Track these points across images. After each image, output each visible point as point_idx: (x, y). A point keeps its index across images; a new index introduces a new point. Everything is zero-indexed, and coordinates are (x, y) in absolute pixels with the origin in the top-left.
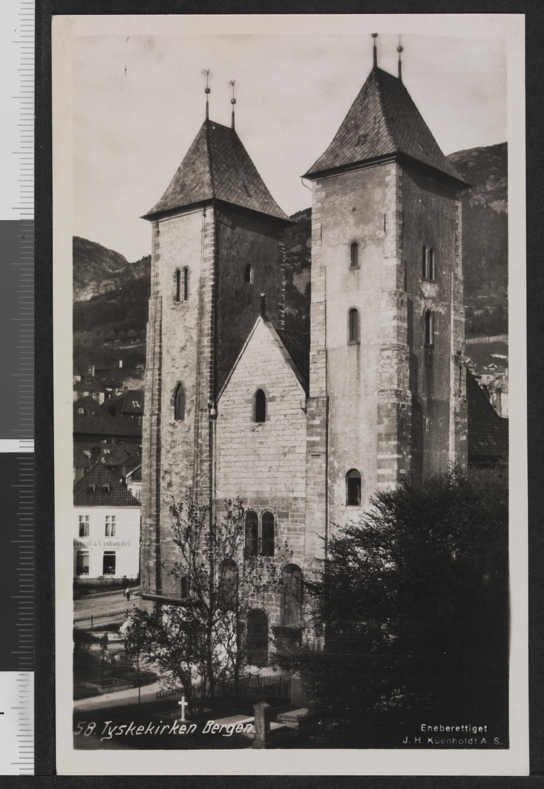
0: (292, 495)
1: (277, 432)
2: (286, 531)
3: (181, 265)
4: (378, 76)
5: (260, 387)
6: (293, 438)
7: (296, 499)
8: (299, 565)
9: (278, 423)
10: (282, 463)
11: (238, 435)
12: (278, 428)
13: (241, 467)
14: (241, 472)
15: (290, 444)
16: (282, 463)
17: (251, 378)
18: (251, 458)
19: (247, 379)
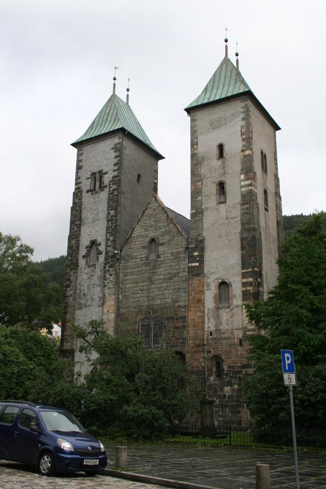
0: (177, 305)
1: (166, 265)
2: (172, 330)
3: (96, 170)
4: (226, 60)
5: (153, 237)
6: (177, 267)
7: (180, 306)
8: (181, 351)
9: (166, 258)
10: (169, 284)
11: (137, 269)
12: (166, 262)
13: (138, 290)
14: (138, 293)
15: (175, 272)
16: (169, 284)
17: (146, 233)
18: (146, 283)
19: (143, 233)
